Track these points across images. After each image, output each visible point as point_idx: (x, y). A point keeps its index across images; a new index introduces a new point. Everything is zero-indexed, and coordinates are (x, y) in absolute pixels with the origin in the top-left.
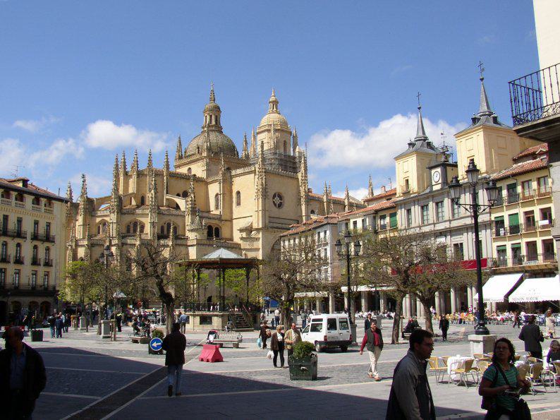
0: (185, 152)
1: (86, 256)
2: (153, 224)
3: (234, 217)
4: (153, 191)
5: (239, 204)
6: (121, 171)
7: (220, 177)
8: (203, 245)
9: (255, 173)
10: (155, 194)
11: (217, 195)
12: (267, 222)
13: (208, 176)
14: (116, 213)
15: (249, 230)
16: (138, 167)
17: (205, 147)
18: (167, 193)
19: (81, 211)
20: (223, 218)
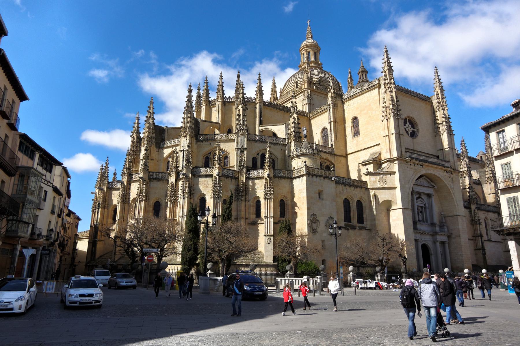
0: (281, 92)
1: (139, 194)
2: (241, 150)
3: (349, 152)
4: (240, 107)
5: (356, 133)
6: (203, 100)
7: (330, 101)
8: (317, 176)
9: (380, 87)
10: (244, 110)
11: (324, 130)
12: (404, 150)
13: (310, 110)
14: (188, 138)
15: (377, 162)
16: (223, 94)
17: (306, 79)
18: (261, 123)
19: (144, 142)
20: (336, 152)
